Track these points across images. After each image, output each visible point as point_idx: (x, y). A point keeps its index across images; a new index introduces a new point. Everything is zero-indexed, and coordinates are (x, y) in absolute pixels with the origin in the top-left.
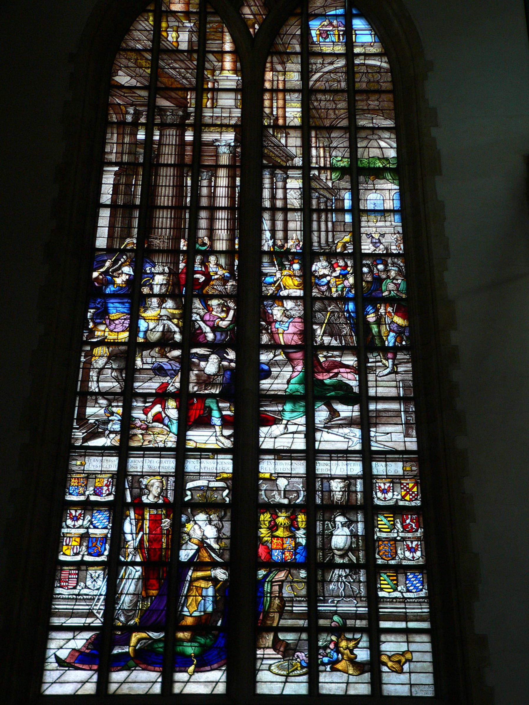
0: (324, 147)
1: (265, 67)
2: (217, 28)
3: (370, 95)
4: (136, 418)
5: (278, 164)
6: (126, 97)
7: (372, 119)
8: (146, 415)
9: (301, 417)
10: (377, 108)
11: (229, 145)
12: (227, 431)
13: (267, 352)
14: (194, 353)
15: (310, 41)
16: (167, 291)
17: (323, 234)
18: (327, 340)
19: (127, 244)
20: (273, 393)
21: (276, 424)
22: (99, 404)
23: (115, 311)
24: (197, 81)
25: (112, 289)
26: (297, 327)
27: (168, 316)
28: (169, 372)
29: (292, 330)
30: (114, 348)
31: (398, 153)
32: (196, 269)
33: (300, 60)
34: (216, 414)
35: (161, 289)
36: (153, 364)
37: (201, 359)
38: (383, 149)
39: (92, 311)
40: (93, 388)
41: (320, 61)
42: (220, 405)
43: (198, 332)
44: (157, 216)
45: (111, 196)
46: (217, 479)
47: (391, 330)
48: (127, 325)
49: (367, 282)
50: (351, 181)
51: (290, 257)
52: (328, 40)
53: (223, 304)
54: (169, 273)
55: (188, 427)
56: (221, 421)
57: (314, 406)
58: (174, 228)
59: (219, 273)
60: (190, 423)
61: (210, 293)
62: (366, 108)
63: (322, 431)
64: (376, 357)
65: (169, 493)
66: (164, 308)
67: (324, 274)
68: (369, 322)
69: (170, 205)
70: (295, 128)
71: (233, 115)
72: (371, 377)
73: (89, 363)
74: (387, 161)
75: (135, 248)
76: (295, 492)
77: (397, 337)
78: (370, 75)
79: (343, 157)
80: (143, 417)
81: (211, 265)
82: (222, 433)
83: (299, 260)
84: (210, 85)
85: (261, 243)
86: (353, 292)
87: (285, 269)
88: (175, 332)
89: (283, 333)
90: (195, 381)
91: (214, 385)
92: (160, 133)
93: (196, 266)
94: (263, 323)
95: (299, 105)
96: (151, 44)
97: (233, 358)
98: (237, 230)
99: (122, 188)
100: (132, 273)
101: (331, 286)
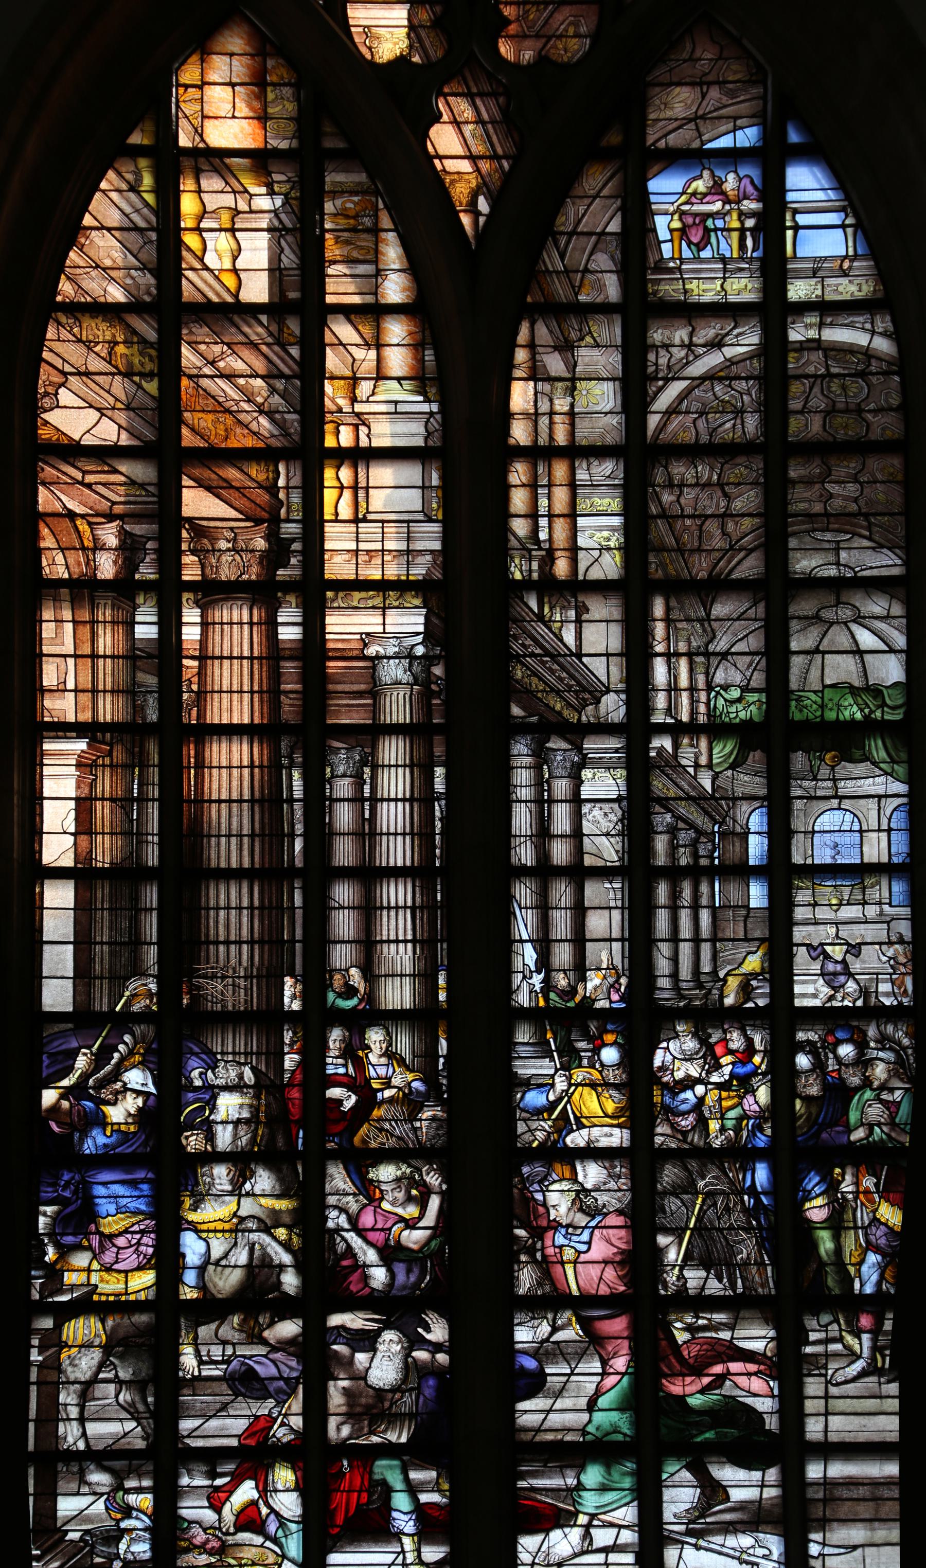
0: (690, 655)
1: (510, 365)
2: (355, 217)
3: (832, 461)
4: (190, 1522)
5: (553, 718)
6: (89, 486)
7: (837, 550)
8: (218, 1510)
9: (625, 1505)
10: (853, 507)
11: (411, 657)
12: (434, 1548)
13: (533, 1318)
14: (337, 1328)
15: (652, 259)
16: (253, 1141)
17: (685, 949)
18: (694, 1277)
19: (134, 996)
20: (550, 1437)
21: (561, 1527)
22: (89, 1484)
23: (112, 1209)
24: (303, 423)
25: (101, 1140)
27: (260, 1220)
28: (273, 1386)
29: (599, 1250)
30: (118, 1320)
31: (909, 668)
32: (330, 1070)
33: (618, 331)
34: (401, 1501)
35: (236, 1137)
36: (228, 1362)
38: (867, 657)
39: (49, 1210)
40: (70, 1440)
41: (681, 334)
42: (414, 1475)
43: (345, 1263)
44: (212, 903)
45: (71, 839)
47: (871, 1247)
48: (150, 1250)
49: (807, 1099)
50: (769, 771)
52: (706, 254)
53: (411, 1178)
54: (258, 1087)
55: (330, 1543)
56: (417, 1520)
57: (660, 1471)
58: (261, 942)
59: (396, 1081)
60: (336, 1530)
61: (373, 1145)
62: (818, 508)
63: (683, 1543)
64: (826, 1326)
66: (248, 1194)
67: (688, 1077)
68: (810, 1221)
69: (246, 864)
70: (602, 587)
71: (418, 545)
72: (813, 1386)
73: (53, 1366)
74: (875, 698)
75: (154, 1008)
77: (886, 1266)
78: (835, 386)
79: (745, 689)
80: (209, 1516)
81: (373, 1058)
82: (419, 1556)
83: (618, 1033)
84: (346, 438)
85: (509, 982)
86: (769, 1132)
87: (580, 1066)
88: (282, 1267)
90: (343, 1409)
92: (202, 616)
93: (329, 1060)
94: (521, 1232)
95: (615, 504)
96: (153, 281)
97: (441, 1340)
98: (442, 941)
99: (103, 812)
100: (153, 1091)
101: (707, 1115)
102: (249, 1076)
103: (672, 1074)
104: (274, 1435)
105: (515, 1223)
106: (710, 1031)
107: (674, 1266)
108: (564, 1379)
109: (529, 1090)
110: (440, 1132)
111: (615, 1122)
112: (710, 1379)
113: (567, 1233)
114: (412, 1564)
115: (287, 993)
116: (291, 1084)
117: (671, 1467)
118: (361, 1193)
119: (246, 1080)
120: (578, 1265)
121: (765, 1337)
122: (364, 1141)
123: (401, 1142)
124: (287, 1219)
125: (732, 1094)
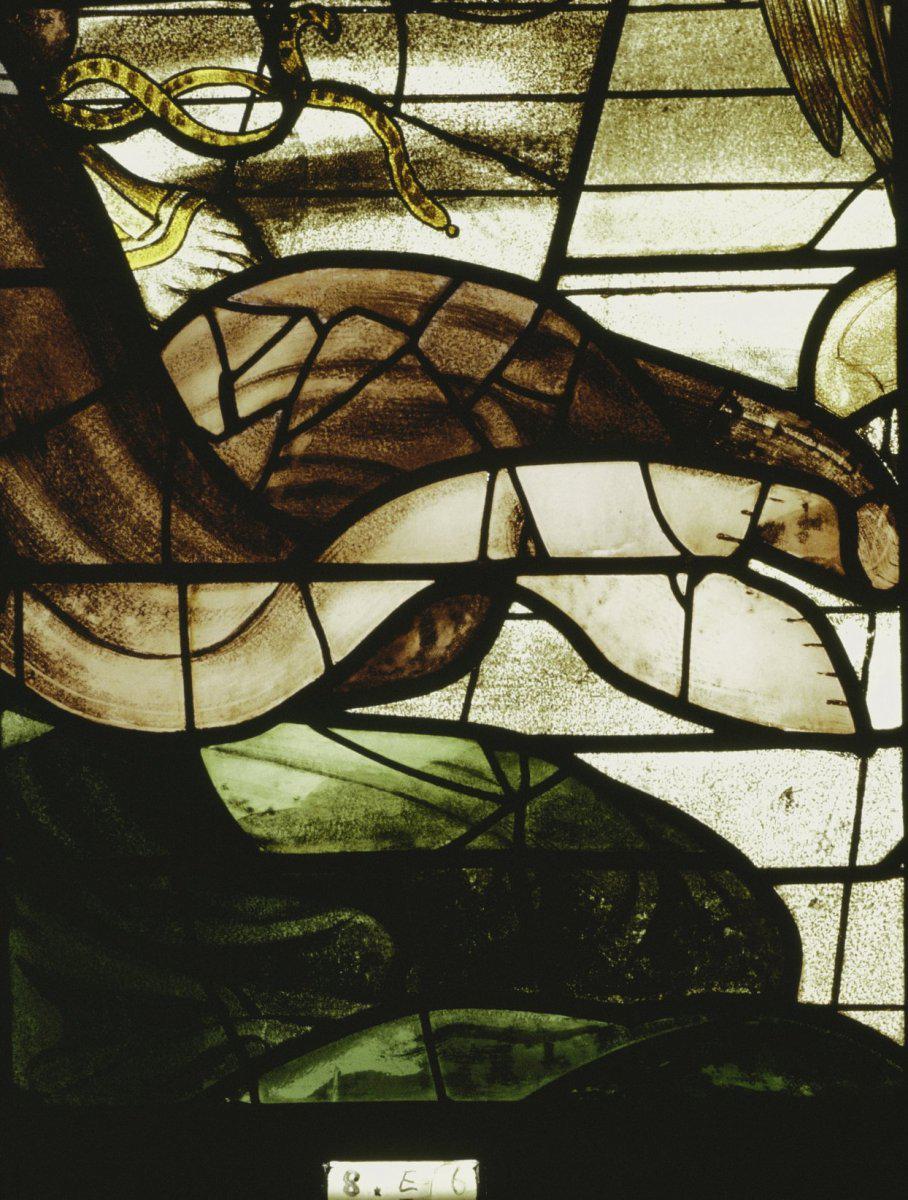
121: (806, 256)
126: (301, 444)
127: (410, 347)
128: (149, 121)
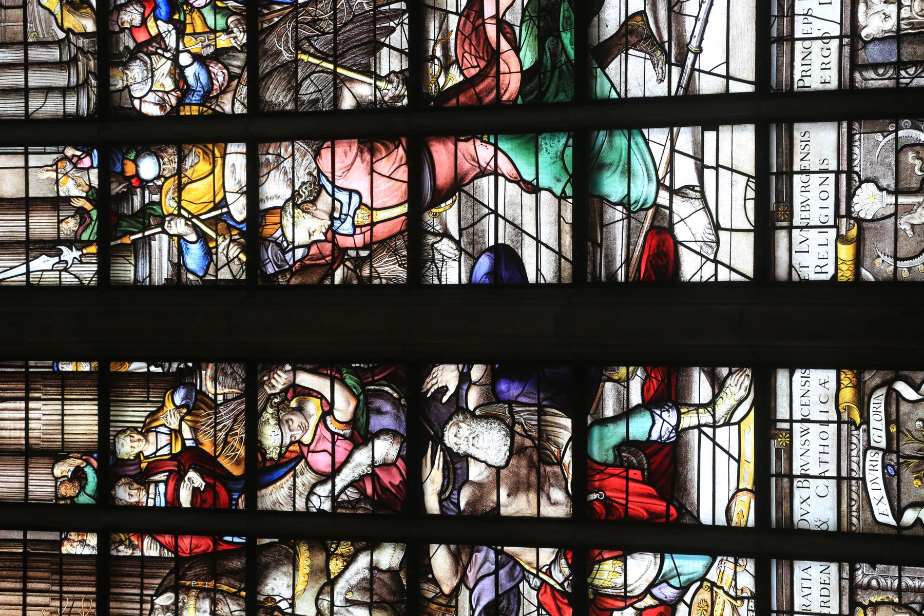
13: (433, 259)
14: (441, 502)
16: (234, 596)
17: (37, 79)
20: (567, 240)
21: (672, 225)
26: (348, 161)
27: (320, 592)
28: (506, 584)
29: (357, 179)
34: (639, 427)
37: (460, 480)
42: (609, 412)
43: (369, 490)
46: (858, 420)
51: (117, 188)
53: (278, 408)
54: (177, 589)
57: (608, 101)
58: (25, 580)
59: (175, 426)
60: (673, 511)
61: (242, 452)
63: (693, 69)
65: (910, 583)
66: (292, 606)
67: (171, 74)
76: (902, 157)
81: (149, 450)
82: (704, 406)
83: (124, 158)
85: (70, 288)
87: (159, 203)
88: (373, 568)
89: (372, 209)
90: (533, 496)
91: (543, 437)
93: (151, 503)
97: (456, 373)
98: (27, 367)
101: (211, 50)
102: (165, 599)
103: (167, 93)
104: (561, 585)
105: (328, 282)
106: (121, 48)
107: (376, 87)
108: (501, 222)
109: (185, 265)
110: (229, 371)
111: (219, 161)
112: (502, 39)
113: (339, 219)
114: (714, 416)
115: (78, 550)
116: (175, 549)
117: (602, 88)
118: (294, 468)
119: (169, 603)
120: (375, 206)
122: (238, 463)
123: (240, 419)
124: (320, 558)
125: (188, 20)
126: (481, 55)
127: (468, 37)
128: (437, 81)
